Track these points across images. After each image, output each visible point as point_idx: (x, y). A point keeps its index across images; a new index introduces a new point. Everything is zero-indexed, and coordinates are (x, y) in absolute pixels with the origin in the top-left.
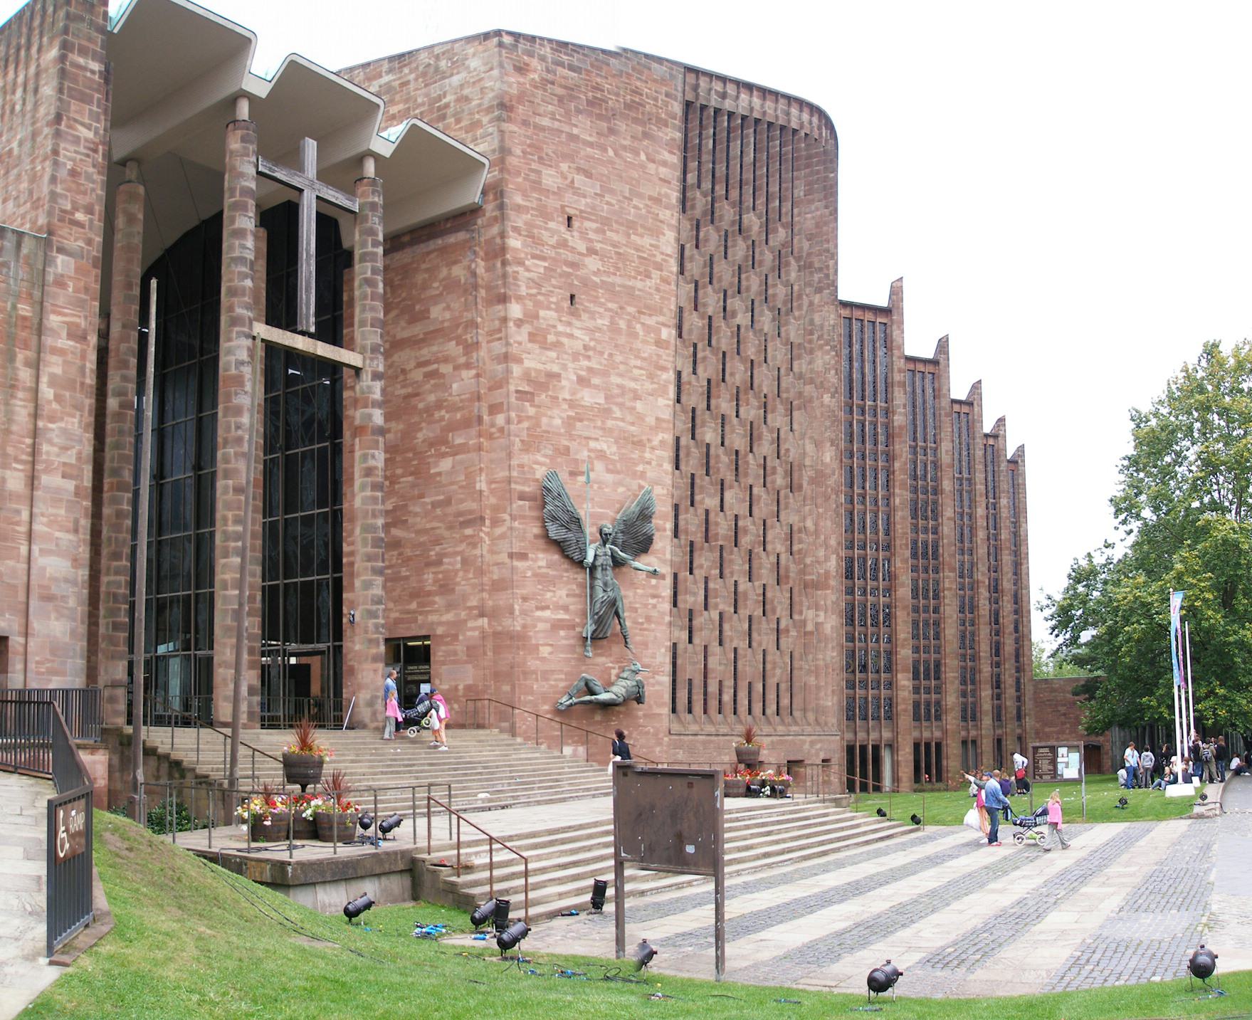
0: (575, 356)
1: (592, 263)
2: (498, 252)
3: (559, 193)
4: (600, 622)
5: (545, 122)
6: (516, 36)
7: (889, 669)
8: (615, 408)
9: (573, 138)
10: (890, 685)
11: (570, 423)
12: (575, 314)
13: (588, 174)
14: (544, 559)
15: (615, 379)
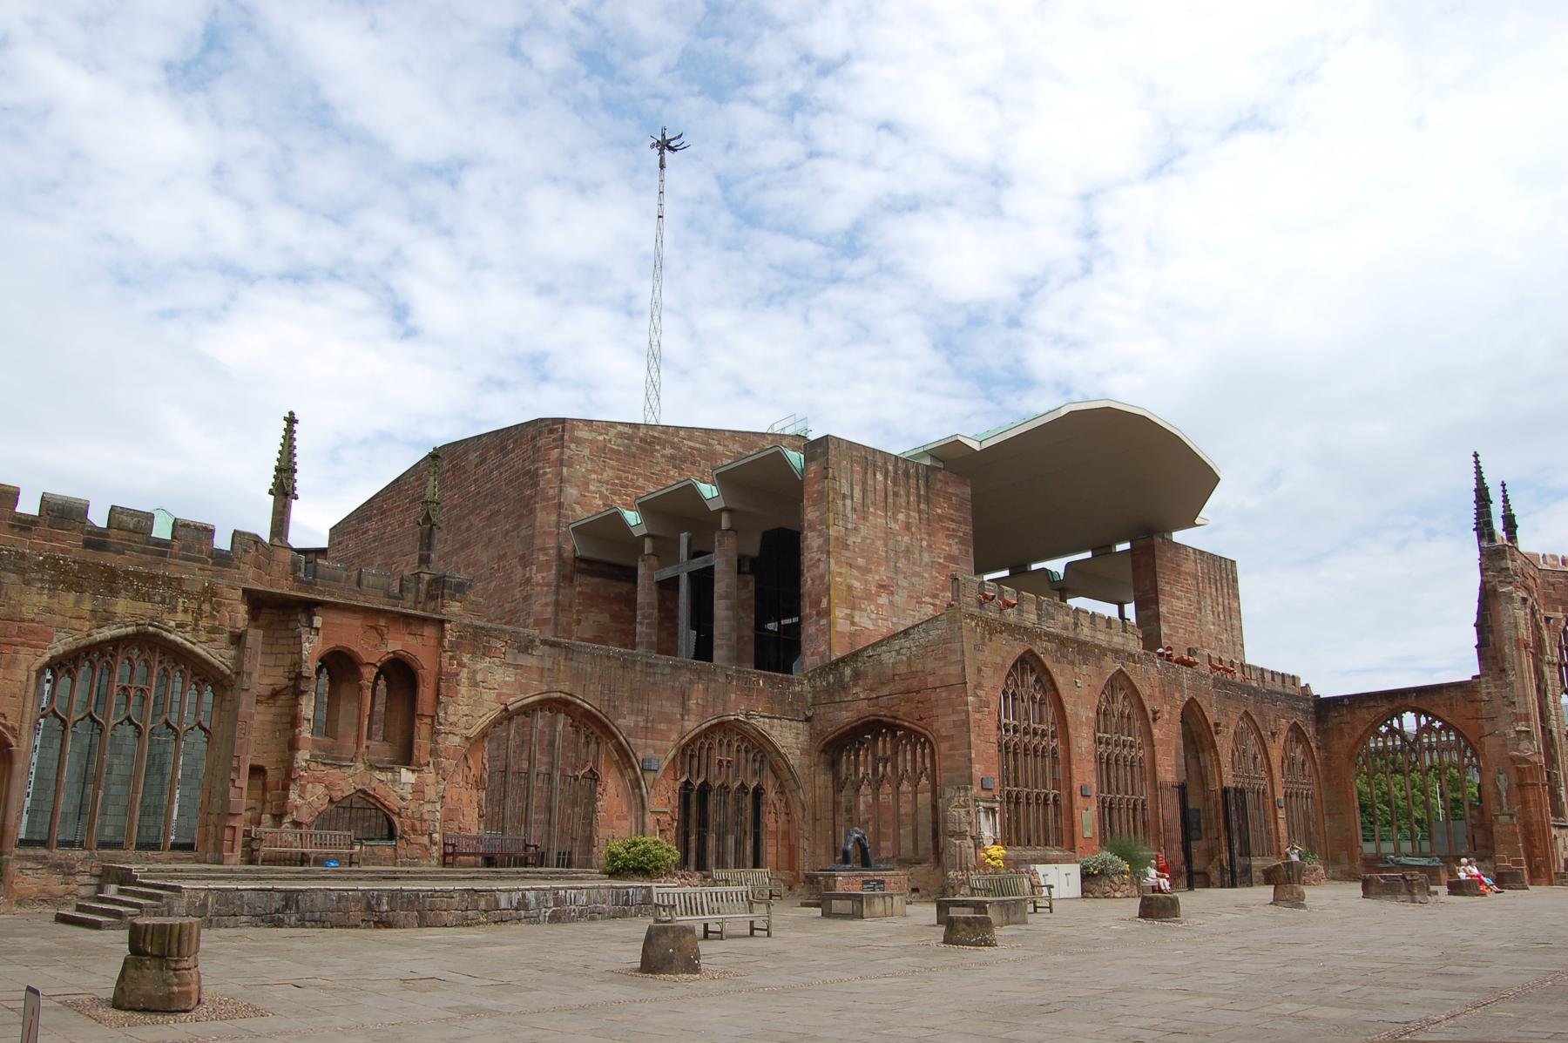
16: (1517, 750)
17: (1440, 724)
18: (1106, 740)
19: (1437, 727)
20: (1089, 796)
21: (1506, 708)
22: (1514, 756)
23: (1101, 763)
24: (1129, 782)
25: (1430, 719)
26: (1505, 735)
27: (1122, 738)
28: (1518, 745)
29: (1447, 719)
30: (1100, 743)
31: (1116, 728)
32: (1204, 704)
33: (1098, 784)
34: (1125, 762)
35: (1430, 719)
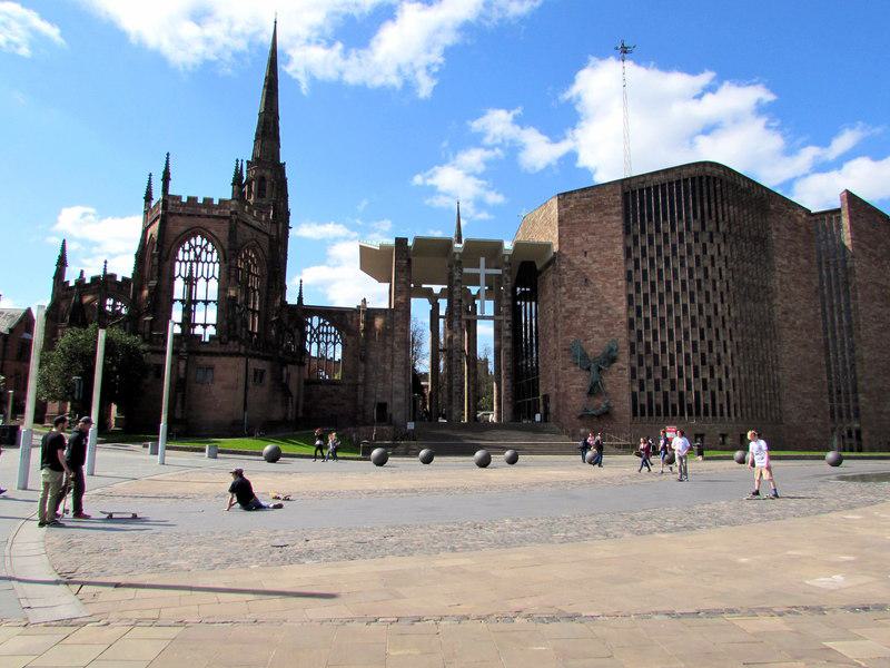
0: (587, 300)
1: (595, 266)
2: (558, 272)
3: (581, 245)
4: (592, 389)
5: (576, 221)
6: (565, 194)
7: (855, 391)
8: (604, 316)
9: (588, 223)
10: (856, 400)
11: (584, 324)
12: (587, 285)
13: (594, 234)
14: (573, 369)
15: (604, 305)
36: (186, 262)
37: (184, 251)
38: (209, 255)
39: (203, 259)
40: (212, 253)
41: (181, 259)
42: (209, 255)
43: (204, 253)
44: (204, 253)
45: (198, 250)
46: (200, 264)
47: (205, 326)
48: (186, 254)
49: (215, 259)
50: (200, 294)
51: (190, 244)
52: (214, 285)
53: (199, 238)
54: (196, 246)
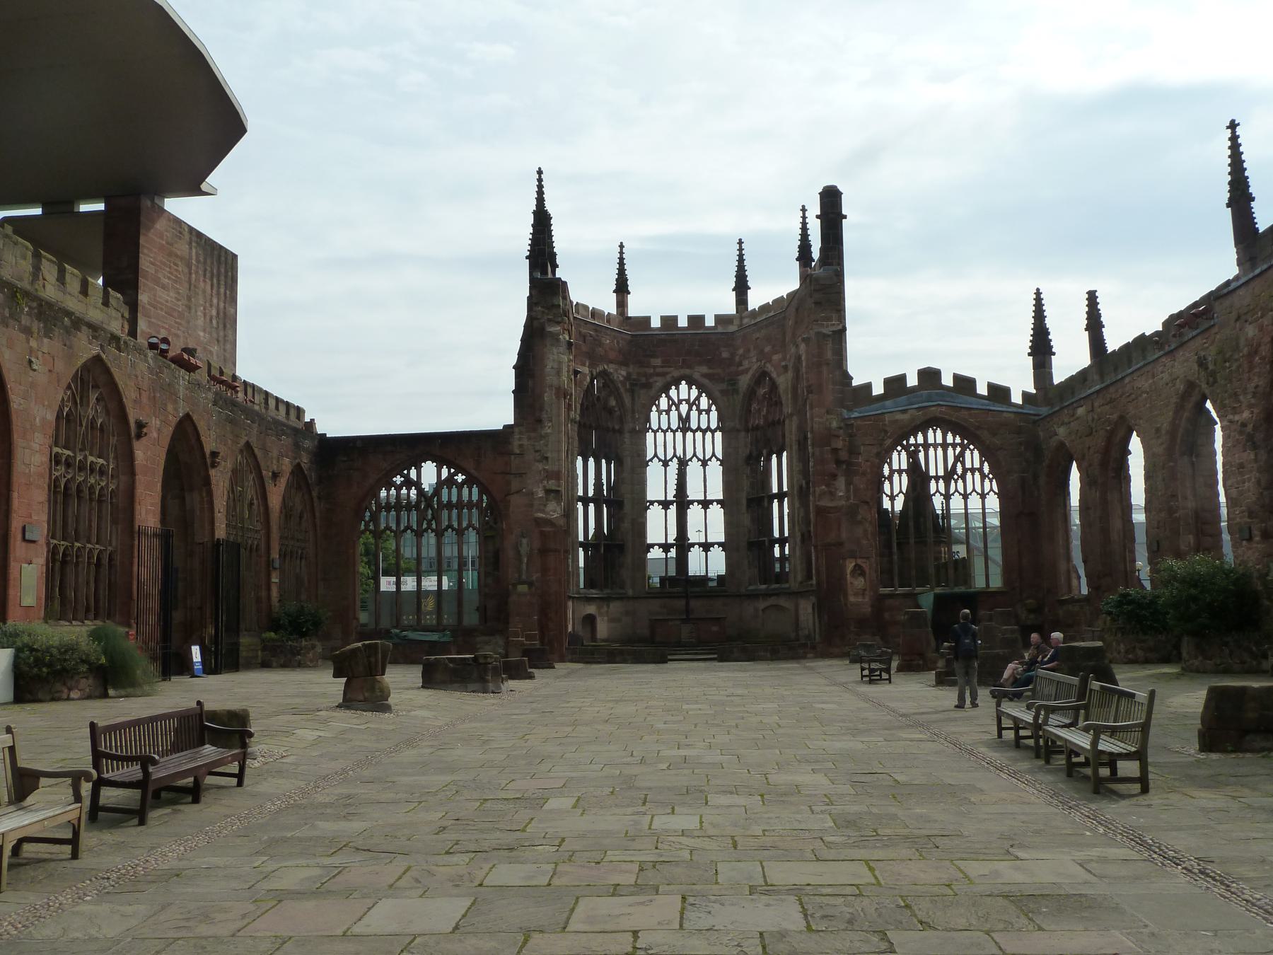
16: (543, 511)
17: (464, 477)
18: (66, 460)
19: (460, 481)
20: (34, 542)
21: (537, 464)
22: (538, 518)
23: (55, 492)
24: (94, 525)
25: (452, 470)
26: (533, 494)
27: (91, 459)
28: (545, 506)
29: (472, 471)
30: (58, 462)
31: (83, 443)
32: (201, 426)
33: (49, 525)
34: (90, 494)
35: (452, 470)
36: (665, 432)
37: (660, 412)
38: (704, 416)
39: (694, 425)
40: (708, 411)
41: (655, 427)
42: (704, 416)
43: (694, 414)
44: (694, 414)
45: (684, 408)
46: (690, 435)
47: (706, 547)
48: (664, 416)
49: (714, 425)
50: (694, 492)
51: (669, 398)
52: (715, 470)
53: (684, 386)
54: (680, 401)
